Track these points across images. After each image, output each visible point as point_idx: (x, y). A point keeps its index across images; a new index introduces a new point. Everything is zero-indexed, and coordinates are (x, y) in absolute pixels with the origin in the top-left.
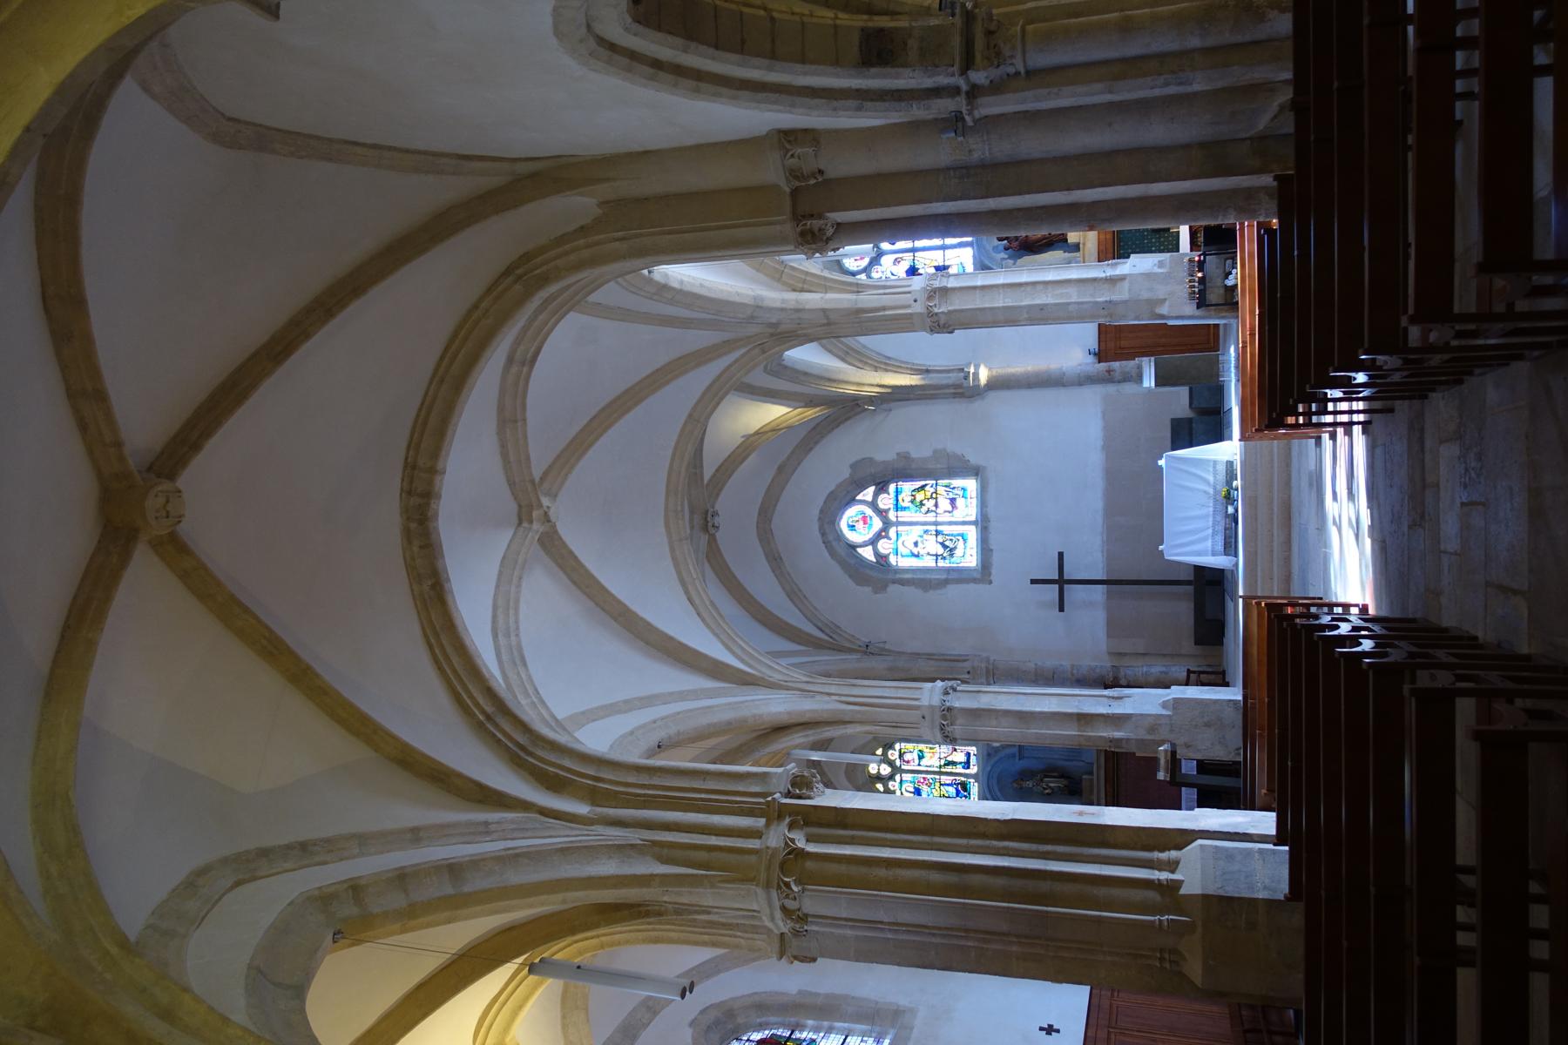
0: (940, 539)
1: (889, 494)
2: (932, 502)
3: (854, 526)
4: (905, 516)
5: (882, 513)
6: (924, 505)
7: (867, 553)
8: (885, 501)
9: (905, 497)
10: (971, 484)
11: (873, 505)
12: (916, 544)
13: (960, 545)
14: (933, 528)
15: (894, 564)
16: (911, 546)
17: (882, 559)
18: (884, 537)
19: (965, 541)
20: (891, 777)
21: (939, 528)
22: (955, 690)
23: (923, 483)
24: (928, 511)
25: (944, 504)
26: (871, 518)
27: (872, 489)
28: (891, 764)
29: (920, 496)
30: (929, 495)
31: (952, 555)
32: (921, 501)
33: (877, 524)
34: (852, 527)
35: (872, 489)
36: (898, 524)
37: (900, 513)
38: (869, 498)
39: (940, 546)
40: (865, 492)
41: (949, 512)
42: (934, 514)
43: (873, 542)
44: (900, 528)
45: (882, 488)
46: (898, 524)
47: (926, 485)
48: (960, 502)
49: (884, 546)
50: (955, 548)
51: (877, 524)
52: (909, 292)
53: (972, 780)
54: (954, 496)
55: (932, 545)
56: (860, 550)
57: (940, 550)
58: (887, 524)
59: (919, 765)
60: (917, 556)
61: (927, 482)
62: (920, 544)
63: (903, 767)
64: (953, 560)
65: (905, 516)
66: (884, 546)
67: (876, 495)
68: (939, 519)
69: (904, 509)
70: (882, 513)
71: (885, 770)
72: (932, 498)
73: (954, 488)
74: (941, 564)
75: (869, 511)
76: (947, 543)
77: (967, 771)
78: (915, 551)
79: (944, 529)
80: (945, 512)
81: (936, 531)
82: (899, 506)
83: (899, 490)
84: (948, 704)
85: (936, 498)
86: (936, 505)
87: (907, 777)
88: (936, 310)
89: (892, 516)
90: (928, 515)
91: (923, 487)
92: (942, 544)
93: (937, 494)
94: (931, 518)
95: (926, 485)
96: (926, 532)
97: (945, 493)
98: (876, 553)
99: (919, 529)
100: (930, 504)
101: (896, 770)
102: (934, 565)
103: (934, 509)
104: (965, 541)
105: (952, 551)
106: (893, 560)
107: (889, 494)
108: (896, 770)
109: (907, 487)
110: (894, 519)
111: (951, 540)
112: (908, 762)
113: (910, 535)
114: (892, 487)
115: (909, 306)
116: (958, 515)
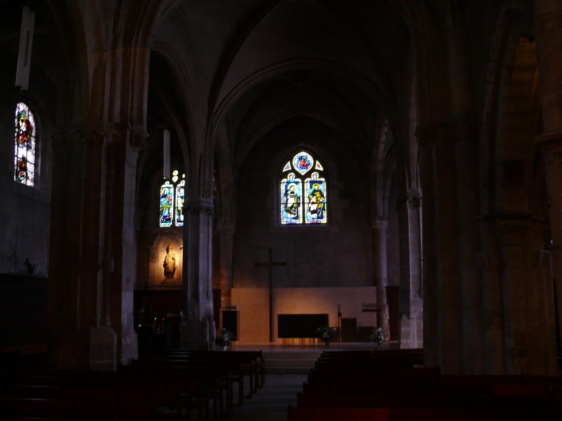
0: (295, 206)
2: (315, 201)
3: (302, 159)
4: (307, 186)
5: (308, 175)
6: (313, 197)
7: (287, 167)
8: (315, 176)
9: (315, 187)
10: (324, 221)
11: (313, 170)
12: (292, 193)
13: (293, 216)
14: (301, 202)
15: (282, 182)
16: (292, 190)
17: (285, 175)
18: (296, 175)
19: (294, 218)
20: (171, 182)
21: (301, 205)
22: (209, 214)
23: (325, 195)
24: (310, 199)
25: (314, 207)
26: (307, 168)
27: (321, 169)
28: (178, 182)
29: (318, 194)
31: (287, 211)
32: (315, 195)
33: (303, 172)
34: (301, 158)
35: (321, 169)
36: (303, 183)
37: (309, 184)
38: (317, 168)
39: (291, 205)
40: (321, 166)
41: (310, 210)
42: (308, 202)
43: (293, 170)
44: (301, 184)
45: (321, 174)
46: (303, 183)
47: (324, 198)
48: (315, 215)
49: (291, 177)
50: (291, 213)
51: (303, 172)
52: (417, 187)
53: (171, 224)
54: (318, 212)
55: (291, 201)
56: (289, 162)
57: (289, 205)
58: (303, 178)
59: (178, 197)
60: (286, 194)
61: (325, 198)
62: (292, 195)
63: (177, 188)
64: (285, 212)
65: (307, 186)
66: (291, 177)
67: (318, 171)
68: (306, 205)
69: (311, 187)
70: (308, 175)
71: (175, 179)
72: (317, 201)
73: (322, 212)
74: (282, 206)
75: (310, 168)
76: (293, 209)
77: (176, 221)
78: (289, 192)
79: (300, 209)
84: (201, 211)
85: (317, 203)
86: (313, 203)
87: (172, 190)
88: (408, 201)
89: (308, 179)
91: (322, 195)
93: (319, 203)
94: (306, 200)
95: (324, 198)
96: (299, 198)
97: (320, 207)
98: (288, 172)
99: (300, 194)
100: (314, 199)
101: (175, 185)
102: (282, 202)
103: (311, 202)
104: (294, 218)
105: (288, 211)
106: (284, 180)
108: (175, 185)
109: (323, 187)
110: (305, 181)
111: (295, 211)
112: (179, 191)
113: (297, 189)
114: (323, 179)
115: (410, 187)
116: (308, 214)
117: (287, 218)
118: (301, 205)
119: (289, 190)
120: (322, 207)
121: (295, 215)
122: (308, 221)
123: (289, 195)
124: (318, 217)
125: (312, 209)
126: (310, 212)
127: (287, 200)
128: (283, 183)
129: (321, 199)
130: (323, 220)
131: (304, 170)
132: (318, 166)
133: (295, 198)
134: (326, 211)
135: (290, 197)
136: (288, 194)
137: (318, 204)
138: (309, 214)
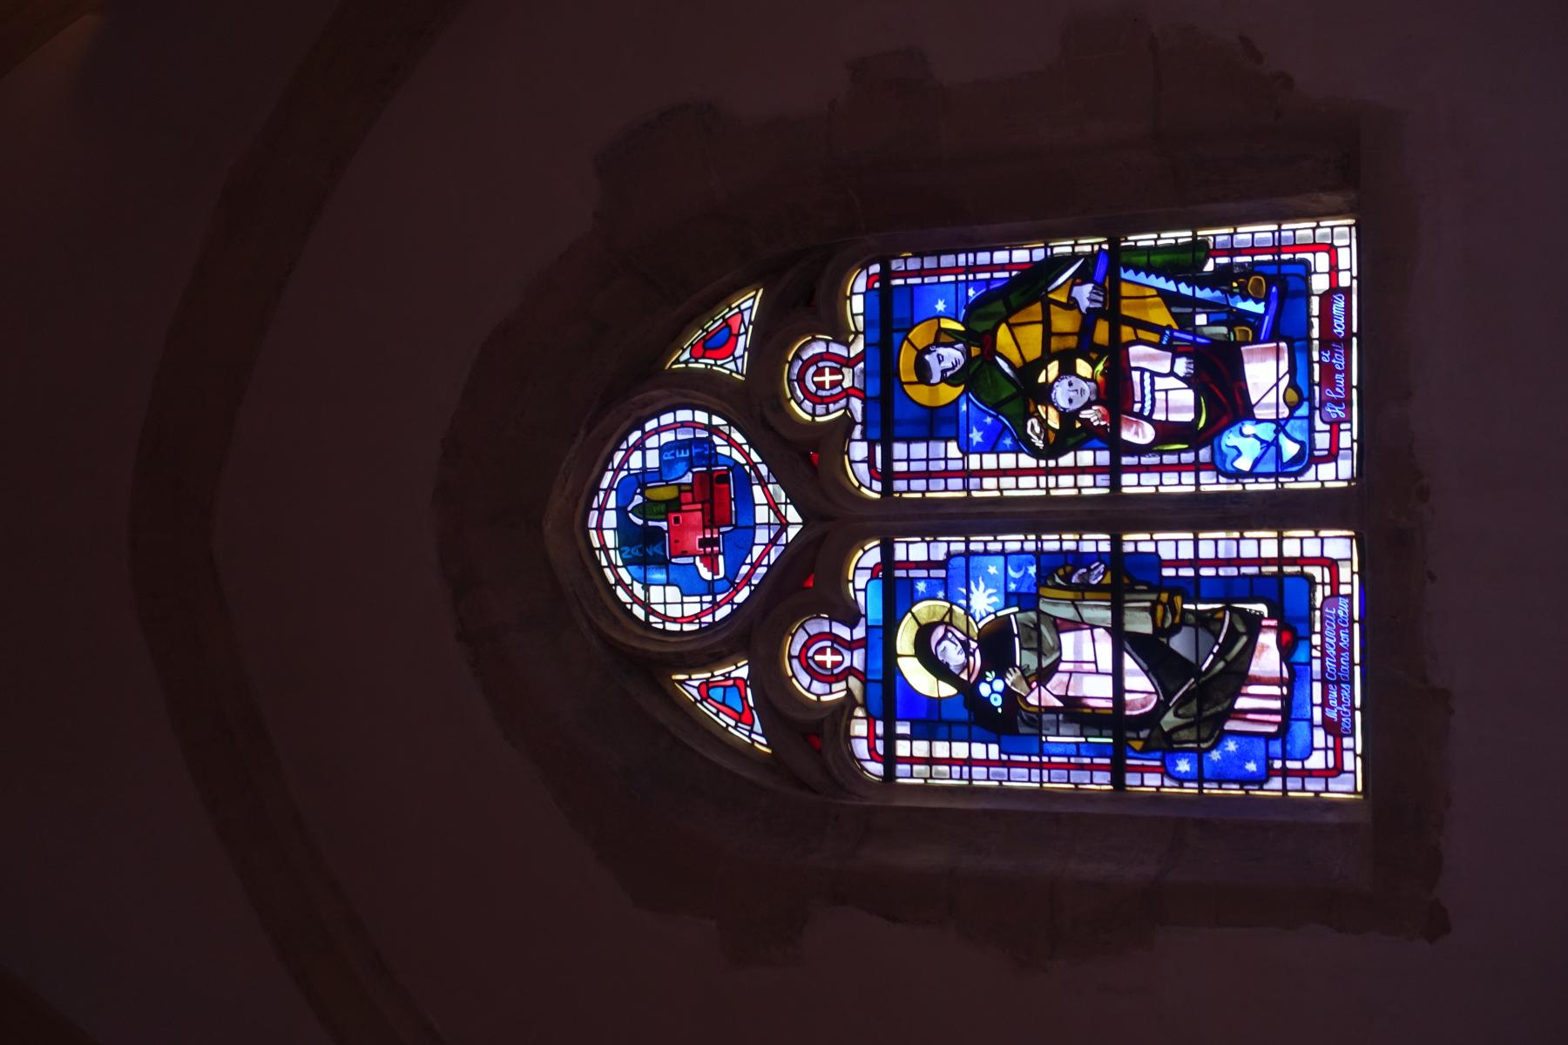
0: (1140, 623)
1: (841, 334)
6: (1045, 394)
14: (1096, 542)
18: (814, 610)
21: (1138, 542)
24: (1072, 434)
30: (1064, 322)
32: (1030, 369)
38: (734, 365)
61: (1063, 248)
69: (937, 424)
72: (1086, 348)
75: (733, 448)
76: (1180, 643)
80: (1168, 432)
81: (1115, 560)
82: (898, 413)
83: (899, 312)
90: (1066, 460)
91: (1034, 281)
92: (1153, 653)
95: (1055, 265)
97: (1161, 316)
107: (841, 334)
110: (873, 492)
117: (1299, 729)
118: (1138, 542)
119: (968, 691)
120: (1161, 283)
121: (1254, 625)
122: (1332, 455)
123: (1021, 689)
124: (1274, 336)
125: (1180, 403)
126: (1230, 439)
127: (1073, 710)
128: (890, 760)
129: (1072, 304)
130: (1321, 261)
131: (762, 514)
132: (720, 344)
133: (1061, 626)
134: (1218, 235)
135: (1043, 676)
136: (1007, 693)
137: (1127, 333)
138: (1244, 445)
